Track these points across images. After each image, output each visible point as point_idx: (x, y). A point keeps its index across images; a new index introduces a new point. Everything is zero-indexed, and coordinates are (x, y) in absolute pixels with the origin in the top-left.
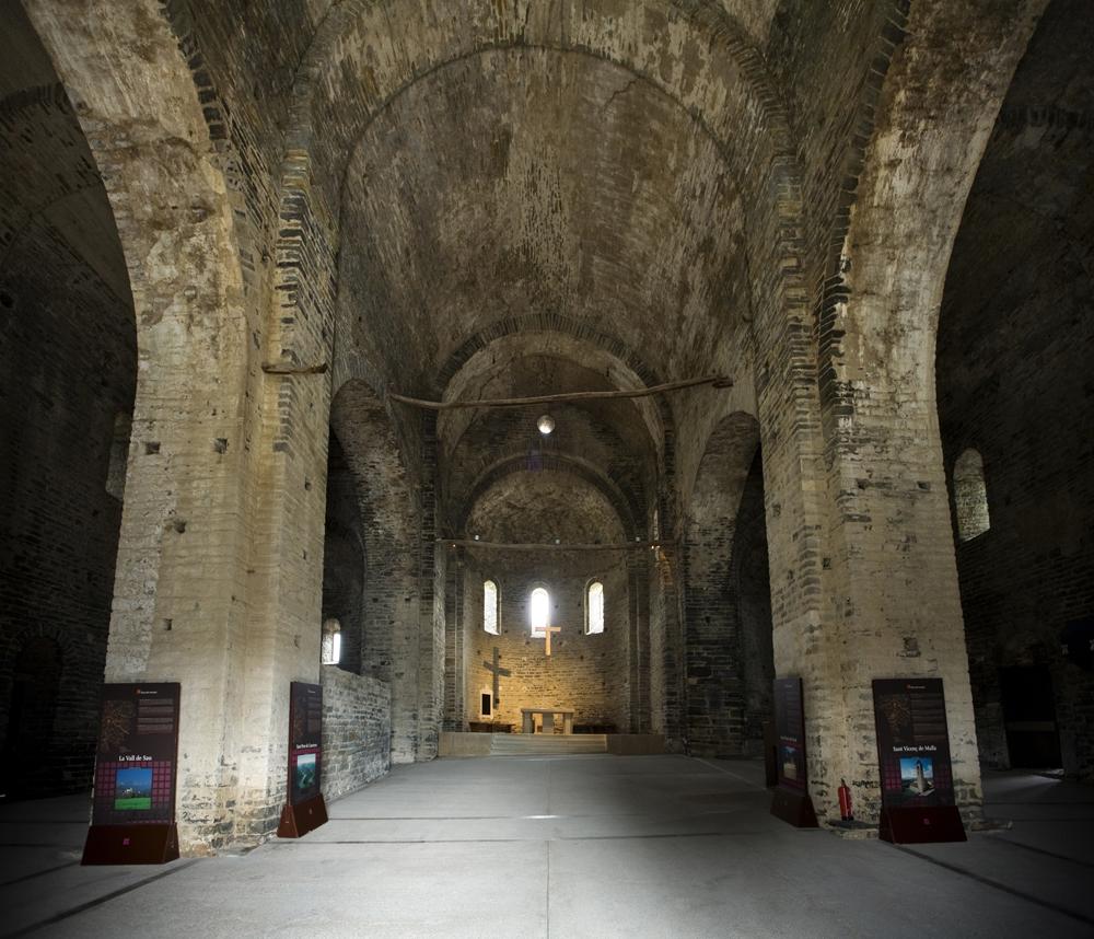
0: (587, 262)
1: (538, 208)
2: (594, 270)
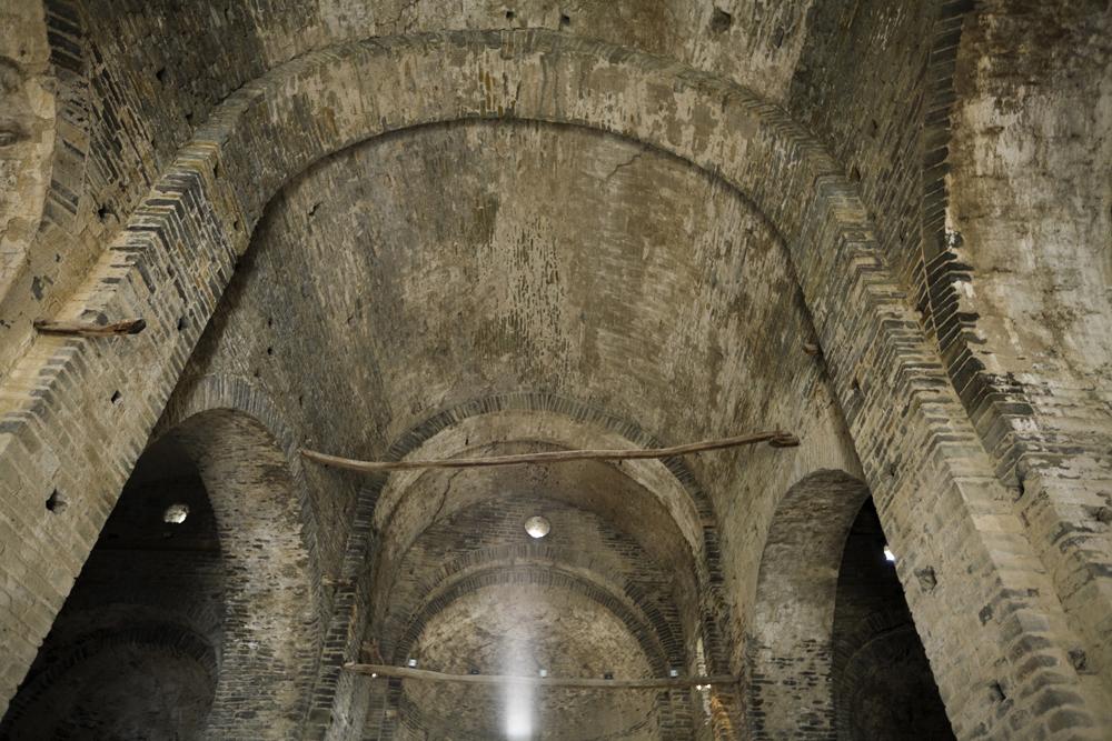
0: (591, 337)
1: (529, 278)
2: (600, 345)
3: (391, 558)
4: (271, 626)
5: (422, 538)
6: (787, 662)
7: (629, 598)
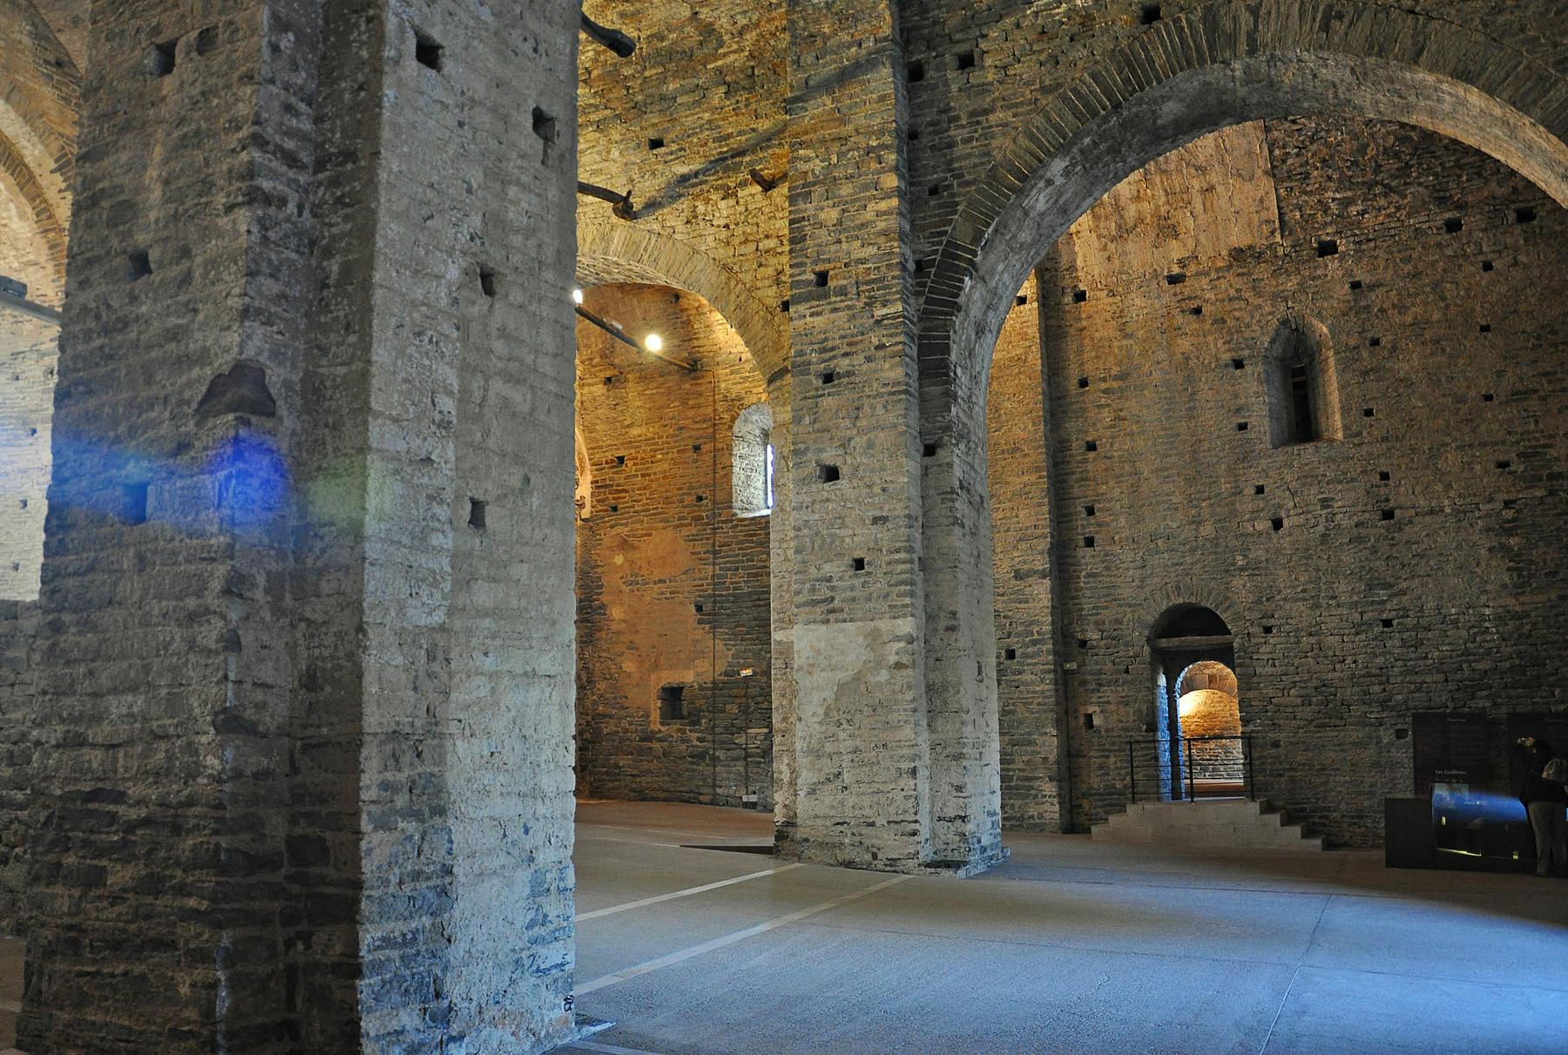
7: (58, 177)
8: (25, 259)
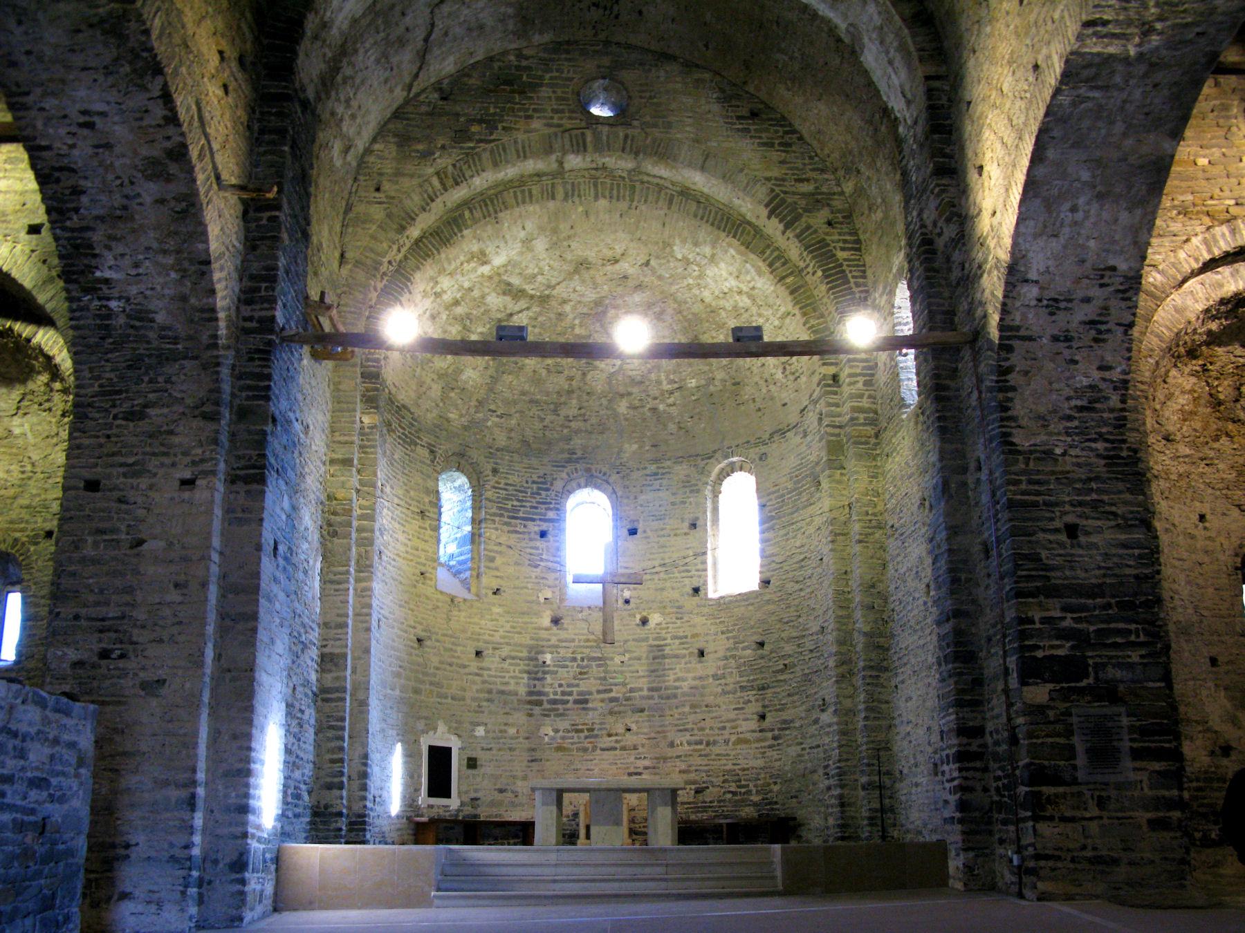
3: (338, 163)
4: (141, 271)
5: (391, 126)
6: (1063, 305)
8: (780, 314)
